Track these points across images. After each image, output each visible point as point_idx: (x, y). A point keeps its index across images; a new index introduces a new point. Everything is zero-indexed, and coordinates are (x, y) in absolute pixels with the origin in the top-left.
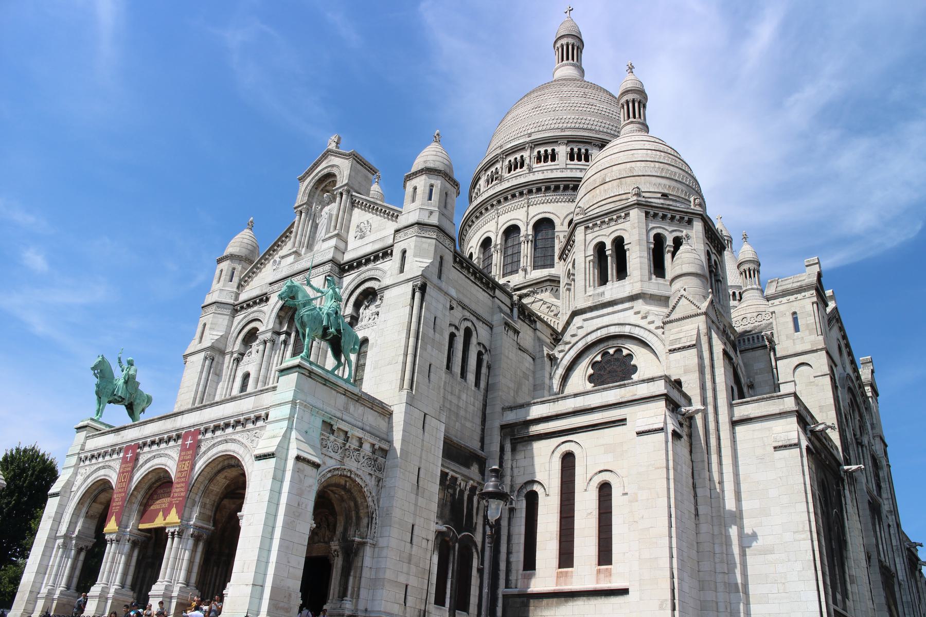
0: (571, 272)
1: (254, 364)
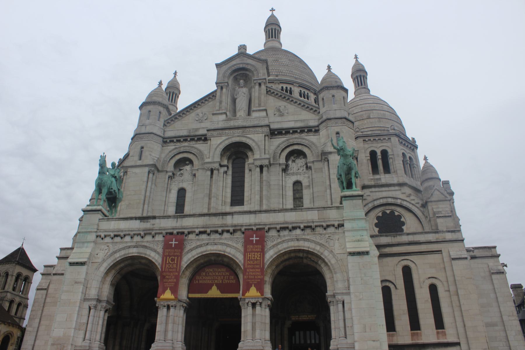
1: (189, 182)
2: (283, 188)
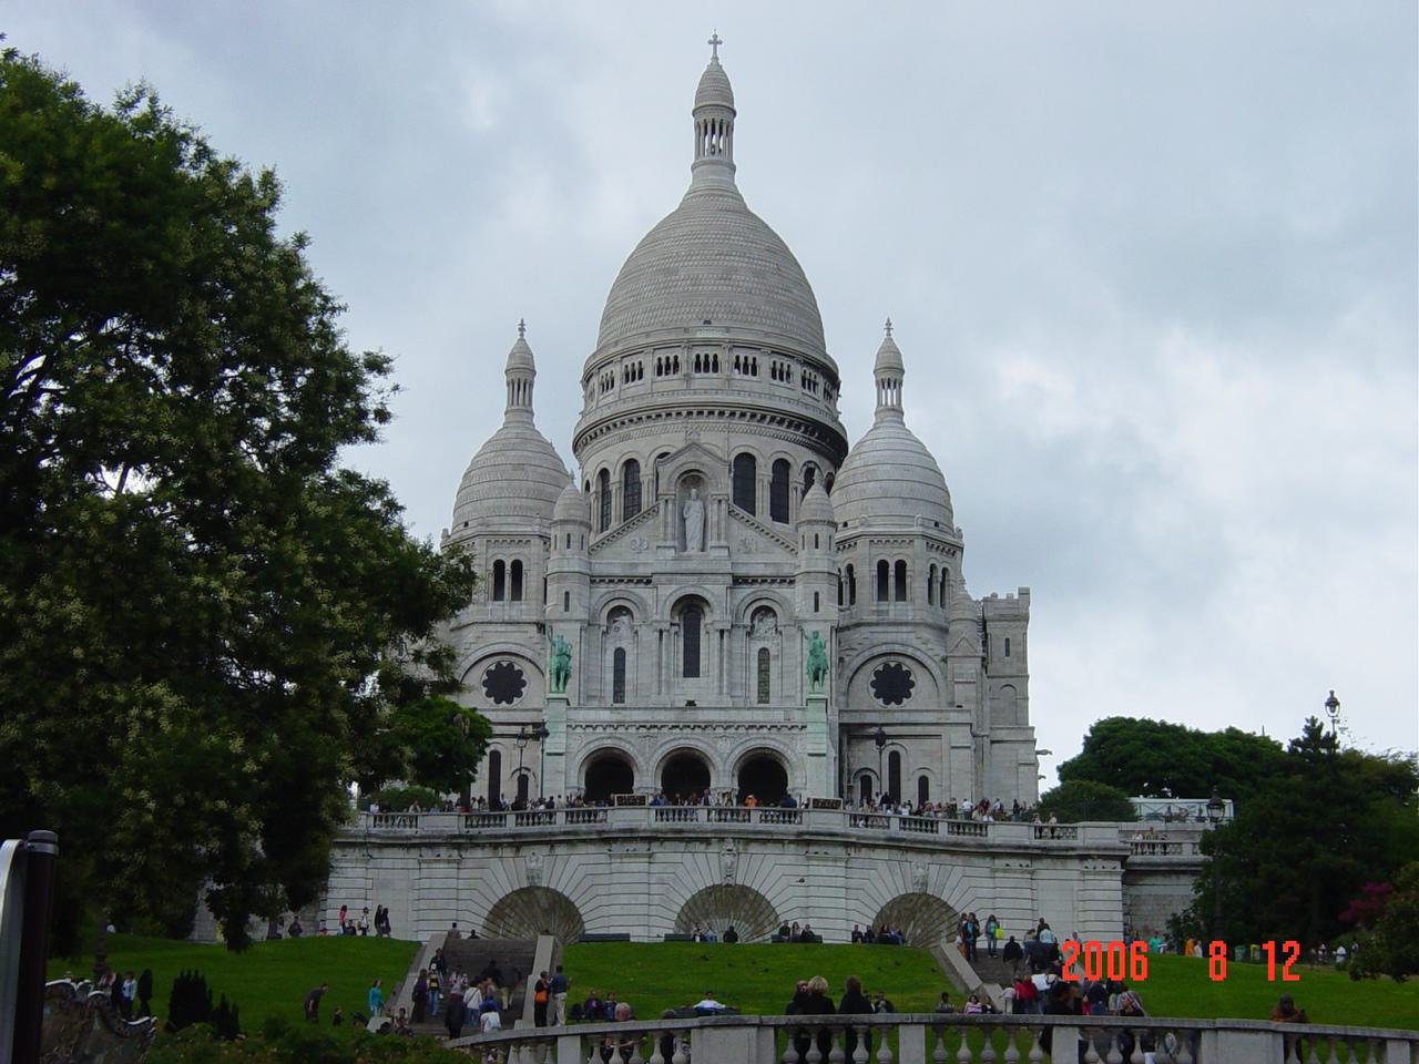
0: (843, 574)
2: (747, 657)
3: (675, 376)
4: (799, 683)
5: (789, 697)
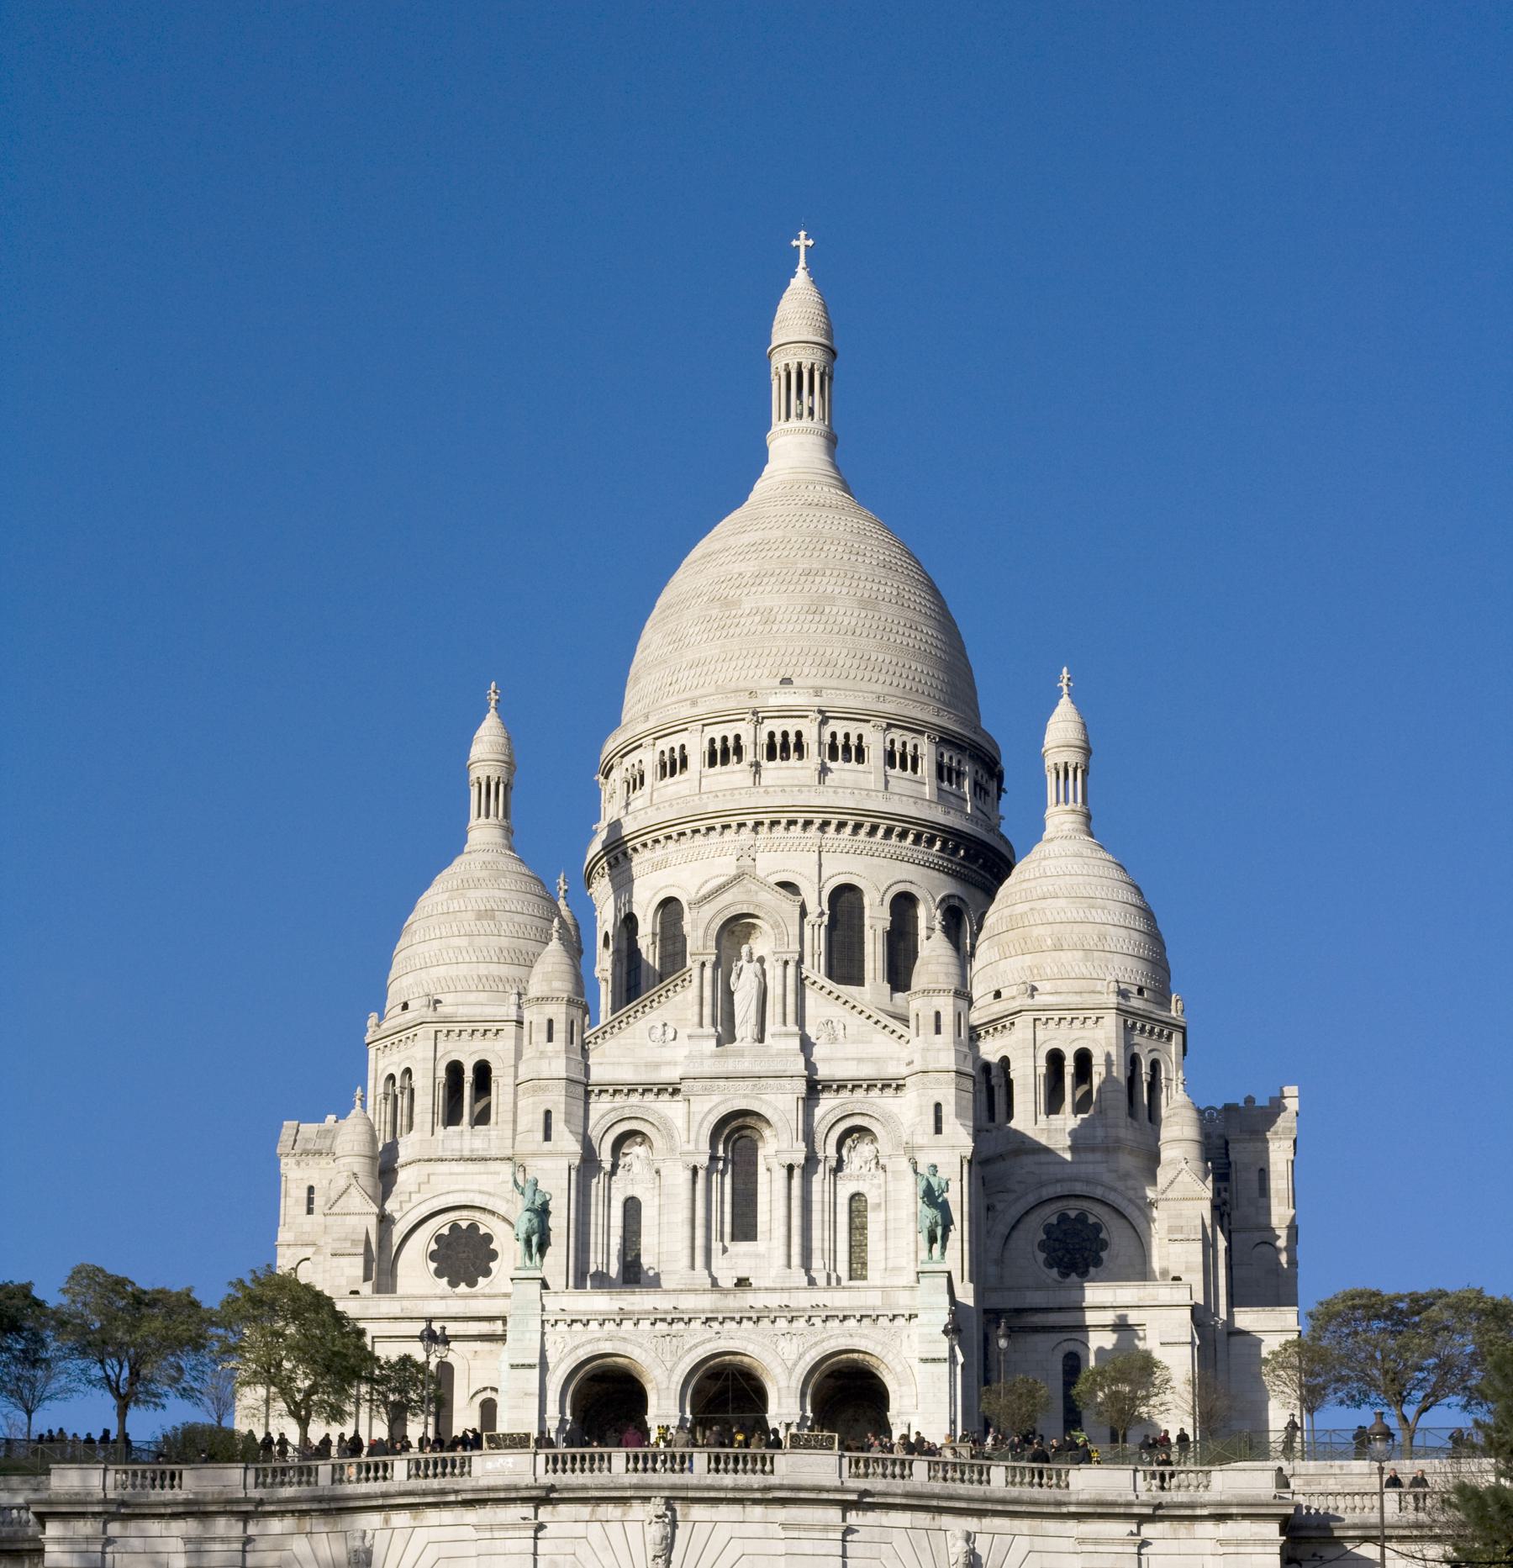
3: (738, 767)
4: (912, 1248)
5: (894, 1269)
